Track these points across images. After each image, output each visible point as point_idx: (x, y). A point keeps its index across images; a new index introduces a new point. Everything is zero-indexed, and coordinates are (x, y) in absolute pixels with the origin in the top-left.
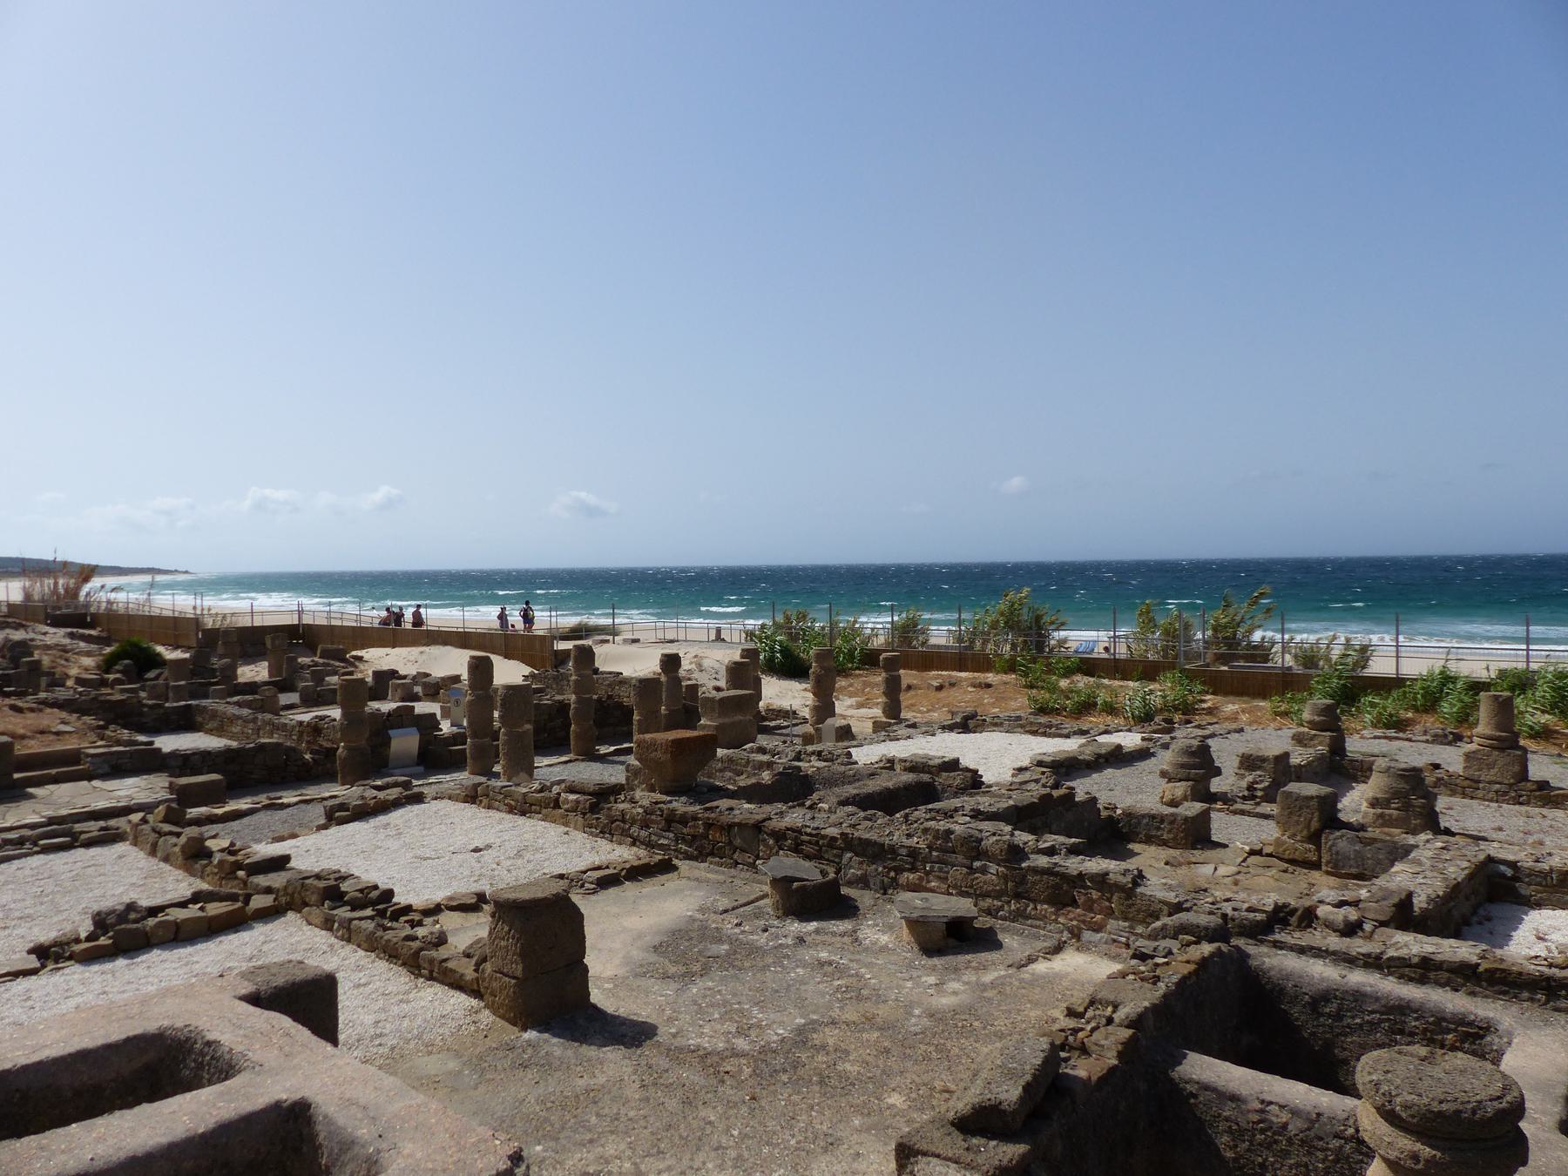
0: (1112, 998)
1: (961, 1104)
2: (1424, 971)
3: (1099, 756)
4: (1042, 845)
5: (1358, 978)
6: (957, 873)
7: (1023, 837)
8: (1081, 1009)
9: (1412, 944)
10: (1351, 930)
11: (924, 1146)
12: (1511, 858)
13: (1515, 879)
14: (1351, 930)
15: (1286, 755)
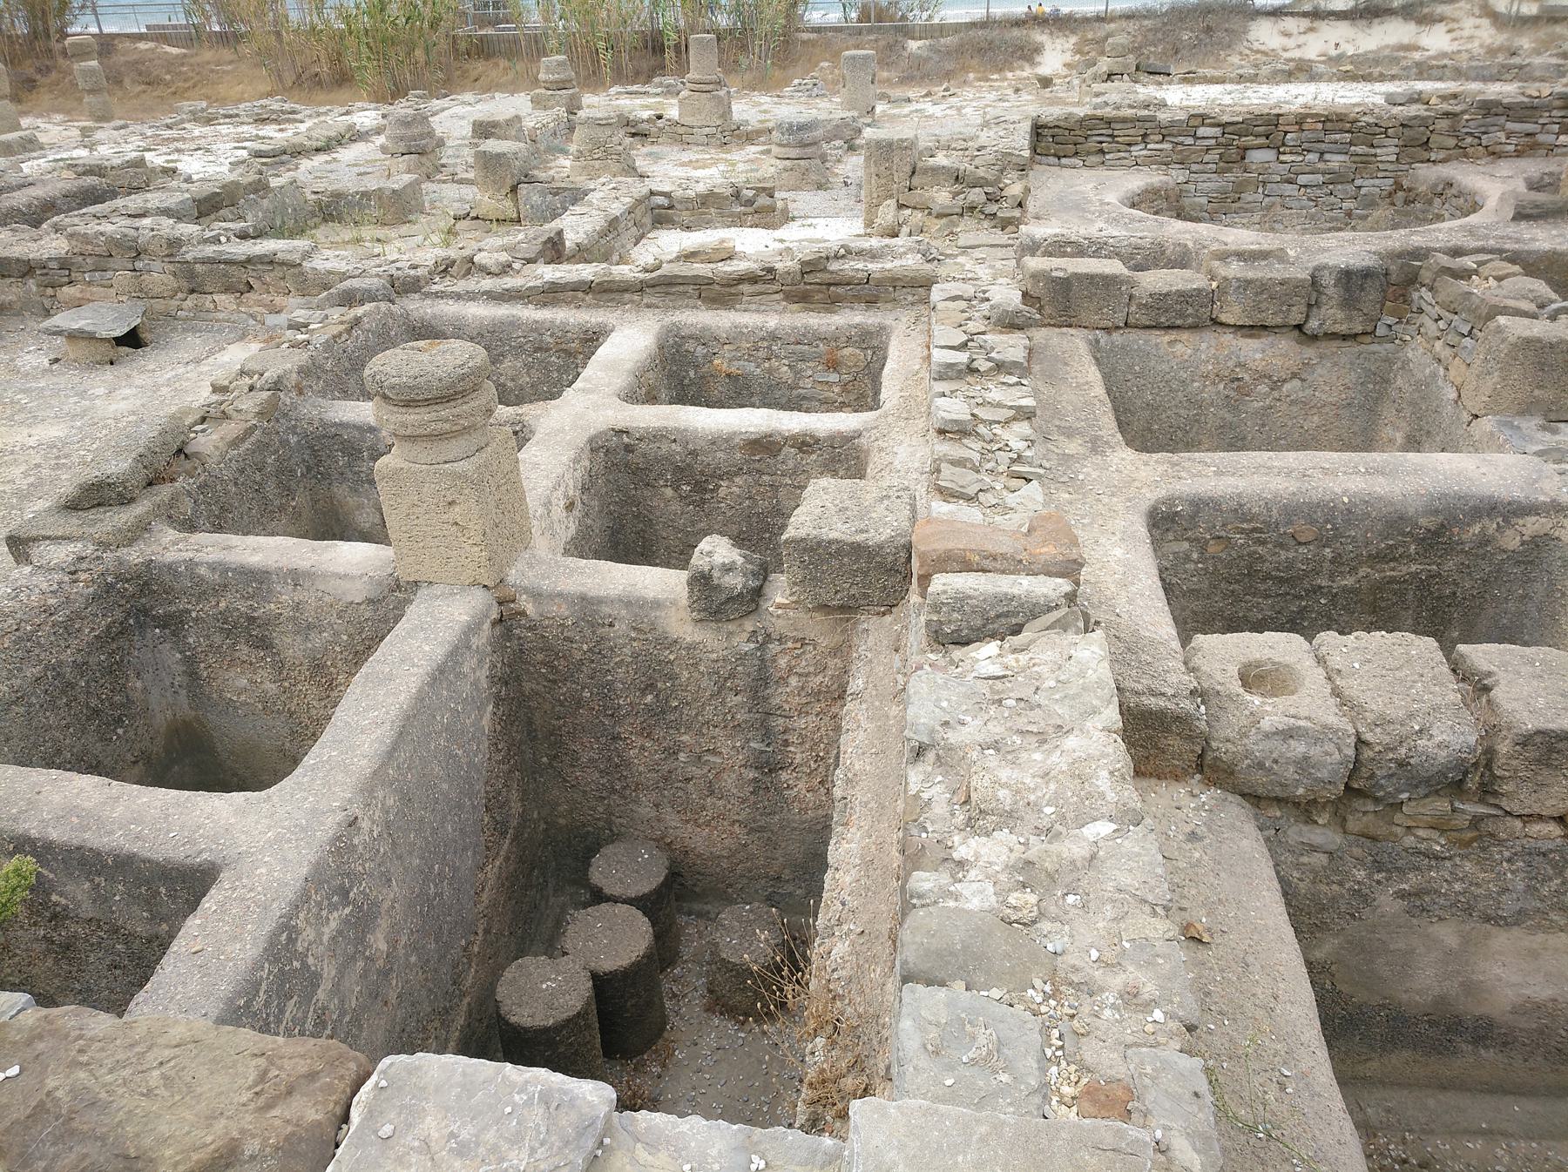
0: (258, 368)
1: (67, 485)
2: (552, 294)
3: (330, 139)
4: (208, 234)
5: (503, 311)
6: (122, 277)
7: (188, 229)
8: (226, 383)
9: (549, 273)
10: (506, 269)
11: (34, 533)
12: (667, 189)
13: (671, 207)
14: (506, 269)
15: (518, 118)
